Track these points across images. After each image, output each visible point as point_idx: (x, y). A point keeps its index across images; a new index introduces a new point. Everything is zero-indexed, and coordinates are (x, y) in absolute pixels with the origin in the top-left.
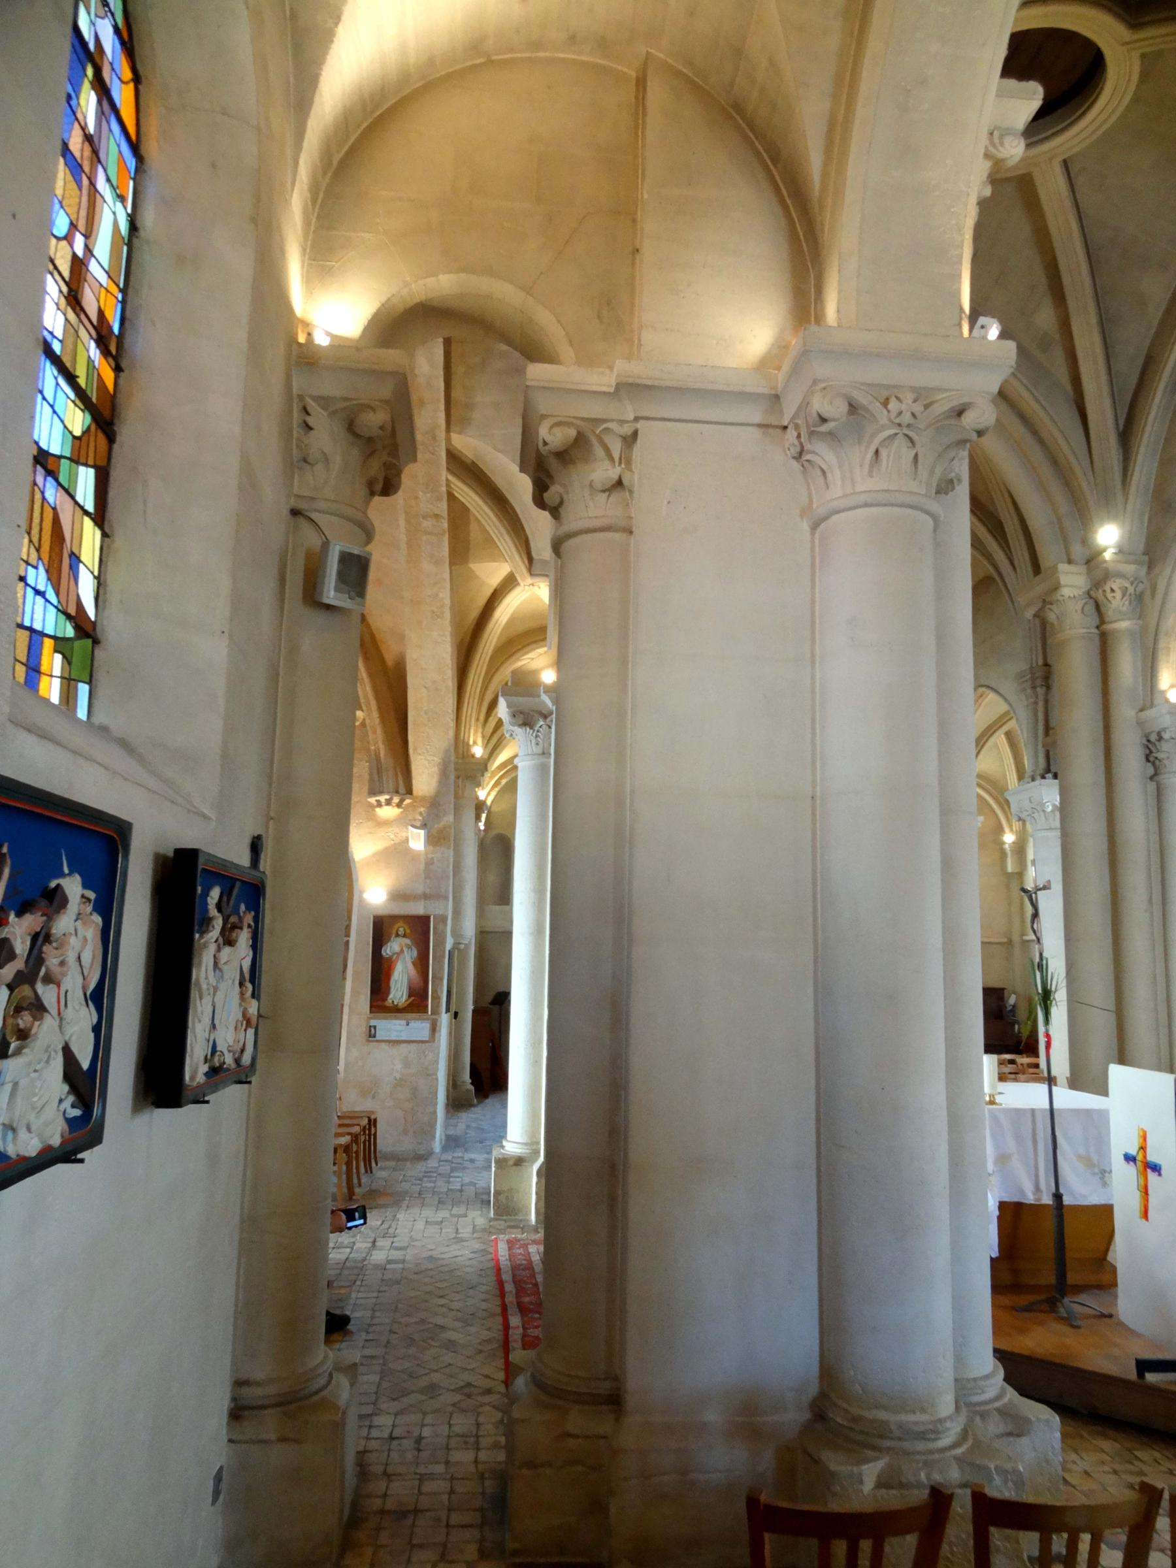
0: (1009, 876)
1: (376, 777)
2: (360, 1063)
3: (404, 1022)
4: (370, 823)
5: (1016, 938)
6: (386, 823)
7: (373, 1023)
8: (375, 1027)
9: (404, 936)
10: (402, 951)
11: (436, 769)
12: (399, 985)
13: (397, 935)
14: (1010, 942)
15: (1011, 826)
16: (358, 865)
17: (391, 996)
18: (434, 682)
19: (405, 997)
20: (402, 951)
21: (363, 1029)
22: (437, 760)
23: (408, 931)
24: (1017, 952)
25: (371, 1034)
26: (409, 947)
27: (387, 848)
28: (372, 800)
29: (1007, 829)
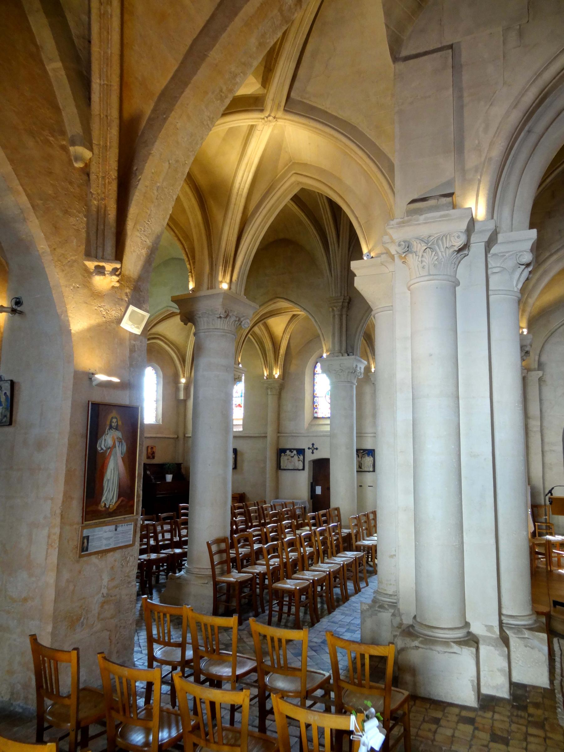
0: (178, 401)
1: (93, 238)
2: (71, 587)
3: (113, 527)
4: (86, 291)
5: (181, 436)
6: (97, 295)
7: (86, 532)
8: (88, 537)
9: (117, 429)
10: (114, 446)
11: (144, 252)
12: (110, 485)
13: (111, 427)
14: (178, 437)
15: (184, 374)
16: (74, 338)
17: (104, 498)
18: (177, 161)
19: (115, 500)
20: (114, 446)
21: (76, 542)
22: (149, 242)
23: (120, 423)
24: (181, 442)
25: (84, 547)
26: (120, 442)
27: (99, 325)
28: (91, 265)
29: (182, 376)
